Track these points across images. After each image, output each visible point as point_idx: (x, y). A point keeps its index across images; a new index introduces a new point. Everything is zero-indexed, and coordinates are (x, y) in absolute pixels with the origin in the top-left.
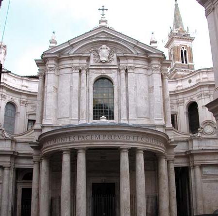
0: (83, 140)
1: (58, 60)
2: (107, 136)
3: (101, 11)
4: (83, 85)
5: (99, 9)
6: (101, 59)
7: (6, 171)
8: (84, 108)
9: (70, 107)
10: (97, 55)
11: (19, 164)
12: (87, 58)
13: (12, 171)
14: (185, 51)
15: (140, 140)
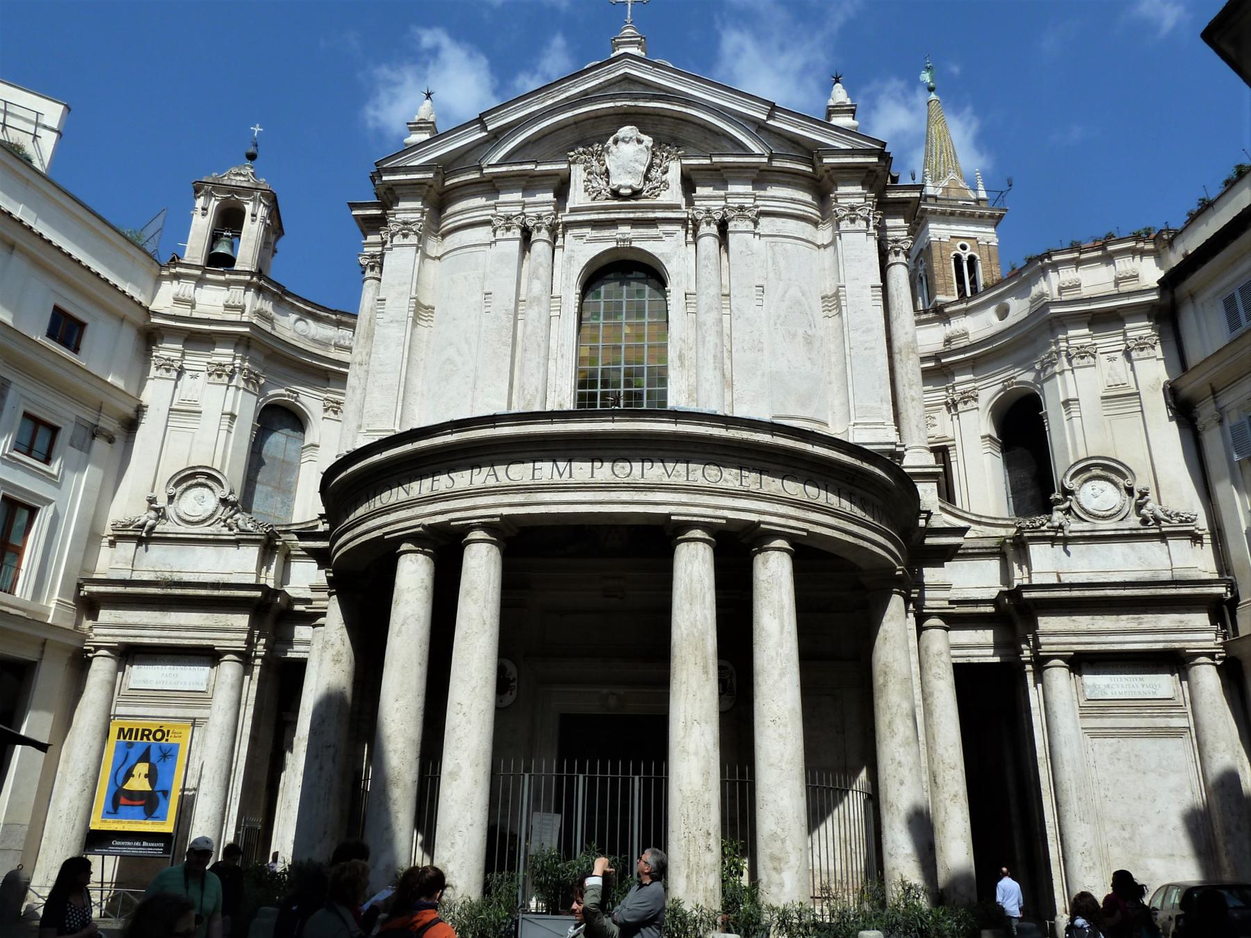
6: (615, 182)
12: (555, 181)
14: (972, 259)
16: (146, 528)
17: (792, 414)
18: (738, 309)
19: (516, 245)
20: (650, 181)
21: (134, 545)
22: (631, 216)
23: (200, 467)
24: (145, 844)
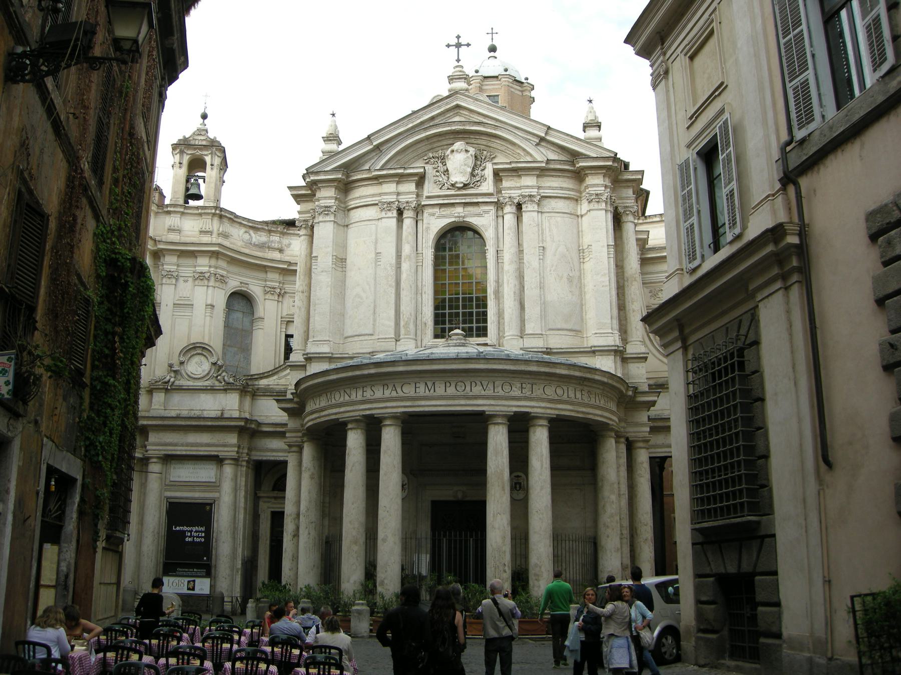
0: (394, 394)
1: (345, 187)
2: (453, 385)
3: (453, 50)
4: (407, 249)
5: (448, 46)
6: (453, 179)
7: (228, 470)
8: (407, 308)
9: (375, 306)
10: (442, 168)
11: (260, 450)
13: (244, 469)
15: (538, 392)
16: (170, 384)
17: (559, 327)
18: (528, 262)
19: (394, 222)
20: (474, 176)
21: (163, 394)
22: (463, 201)
23: (197, 343)
24: (195, 570)
